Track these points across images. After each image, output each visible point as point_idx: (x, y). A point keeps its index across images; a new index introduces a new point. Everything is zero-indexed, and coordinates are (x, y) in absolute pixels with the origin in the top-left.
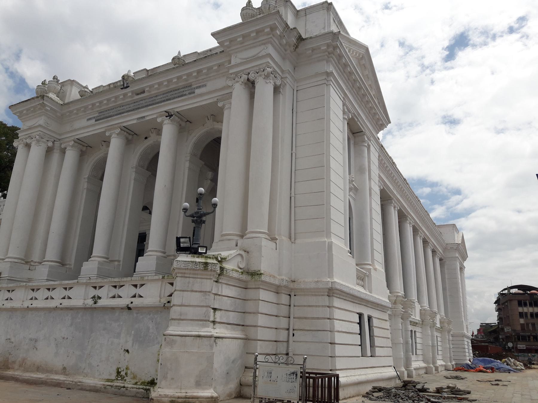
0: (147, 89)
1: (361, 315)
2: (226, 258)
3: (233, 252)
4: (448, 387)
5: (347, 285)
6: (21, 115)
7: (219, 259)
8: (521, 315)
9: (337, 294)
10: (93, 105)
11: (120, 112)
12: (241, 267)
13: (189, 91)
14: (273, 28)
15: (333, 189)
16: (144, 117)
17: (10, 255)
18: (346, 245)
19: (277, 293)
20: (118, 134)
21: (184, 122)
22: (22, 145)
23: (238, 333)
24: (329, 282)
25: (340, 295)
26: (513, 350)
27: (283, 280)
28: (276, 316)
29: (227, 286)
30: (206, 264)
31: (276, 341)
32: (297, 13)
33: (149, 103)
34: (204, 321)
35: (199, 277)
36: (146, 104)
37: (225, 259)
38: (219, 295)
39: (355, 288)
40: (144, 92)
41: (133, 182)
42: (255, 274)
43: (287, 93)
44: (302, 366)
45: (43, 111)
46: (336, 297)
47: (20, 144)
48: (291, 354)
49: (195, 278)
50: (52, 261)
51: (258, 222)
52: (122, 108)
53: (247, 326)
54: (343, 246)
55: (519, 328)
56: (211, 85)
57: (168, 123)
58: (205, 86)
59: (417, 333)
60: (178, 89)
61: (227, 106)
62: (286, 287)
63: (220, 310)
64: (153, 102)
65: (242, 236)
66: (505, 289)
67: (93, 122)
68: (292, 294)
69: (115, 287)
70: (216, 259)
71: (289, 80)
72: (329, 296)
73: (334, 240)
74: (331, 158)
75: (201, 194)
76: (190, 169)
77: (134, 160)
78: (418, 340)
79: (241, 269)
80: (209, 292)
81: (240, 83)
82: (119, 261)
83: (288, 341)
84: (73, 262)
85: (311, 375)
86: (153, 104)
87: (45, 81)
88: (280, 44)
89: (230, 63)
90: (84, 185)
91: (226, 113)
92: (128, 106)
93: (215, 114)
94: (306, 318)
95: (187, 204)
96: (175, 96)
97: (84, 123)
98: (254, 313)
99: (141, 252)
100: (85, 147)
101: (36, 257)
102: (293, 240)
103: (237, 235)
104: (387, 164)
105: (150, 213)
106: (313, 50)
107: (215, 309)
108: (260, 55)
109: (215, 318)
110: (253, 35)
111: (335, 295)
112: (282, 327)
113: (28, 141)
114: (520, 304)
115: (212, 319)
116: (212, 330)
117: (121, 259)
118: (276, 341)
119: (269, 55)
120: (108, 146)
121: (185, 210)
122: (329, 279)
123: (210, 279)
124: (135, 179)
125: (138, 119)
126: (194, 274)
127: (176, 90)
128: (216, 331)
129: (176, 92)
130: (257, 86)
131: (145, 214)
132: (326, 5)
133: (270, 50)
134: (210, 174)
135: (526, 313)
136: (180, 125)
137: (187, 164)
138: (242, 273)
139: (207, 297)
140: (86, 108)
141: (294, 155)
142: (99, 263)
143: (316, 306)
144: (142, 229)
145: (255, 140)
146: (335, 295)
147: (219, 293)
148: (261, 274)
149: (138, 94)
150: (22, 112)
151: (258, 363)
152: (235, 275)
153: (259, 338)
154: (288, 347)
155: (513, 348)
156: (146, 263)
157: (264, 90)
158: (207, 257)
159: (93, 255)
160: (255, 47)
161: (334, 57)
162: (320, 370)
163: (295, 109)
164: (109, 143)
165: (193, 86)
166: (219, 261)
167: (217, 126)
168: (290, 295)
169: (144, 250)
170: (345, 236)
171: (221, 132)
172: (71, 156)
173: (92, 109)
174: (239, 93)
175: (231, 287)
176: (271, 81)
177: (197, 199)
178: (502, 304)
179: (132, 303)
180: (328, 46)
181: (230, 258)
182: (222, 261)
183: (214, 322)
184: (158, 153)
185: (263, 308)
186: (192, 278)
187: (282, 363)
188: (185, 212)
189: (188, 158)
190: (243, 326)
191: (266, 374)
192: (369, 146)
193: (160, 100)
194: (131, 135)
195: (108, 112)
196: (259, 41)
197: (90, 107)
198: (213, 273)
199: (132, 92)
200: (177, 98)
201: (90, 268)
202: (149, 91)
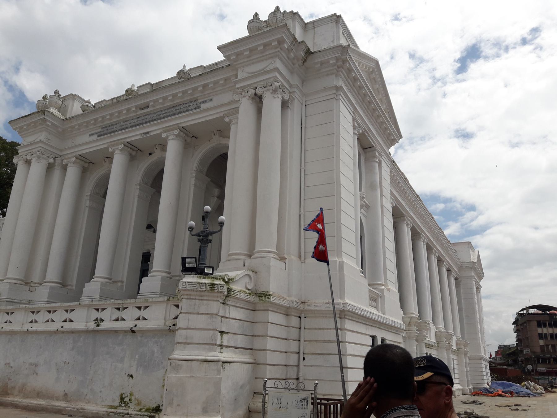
0: (151, 104)
2: (233, 279)
3: (241, 273)
4: (466, 413)
5: (359, 306)
6: (20, 131)
7: (227, 280)
8: (541, 336)
9: (349, 316)
10: (96, 120)
11: (123, 127)
12: (249, 288)
13: (195, 106)
14: (281, 42)
15: (344, 206)
16: (148, 133)
17: (9, 276)
18: (357, 264)
19: (287, 315)
20: (121, 150)
22: (22, 161)
23: (246, 358)
24: (340, 303)
25: (352, 317)
26: (532, 373)
27: (292, 301)
28: (286, 339)
29: (235, 308)
30: (213, 285)
31: (285, 366)
32: (305, 26)
34: (211, 345)
35: (205, 298)
36: (150, 119)
37: (232, 279)
38: (227, 318)
39: (367, 309)
40: (148, 107)
41: (136, 199)
42: (263, 295)
43: (296, 107)
44: (313, 392)
45: (44, 126)
46: (348, 319)
47: (19, 161)
48: (301, 379)
49: (202, 300)
51: (267, 241)
52: (125, 123)
53: (256, 350)
54: (355, 266)
55: (538, 350)
56: (217, 100)
57: (173, 139)
58: (211, 100)
60: (184, 104)
61: (234, 121)
62: (295, 308)
63: (228, 333)
64: (159, 117)
65: (250, 256)
66: (523, 309)
67: (95, 137)
68: (303, 316)
69: (118, 309)
70: (223, 279)
71: (297, 95)
72: (341, 318)
73: (345, 259)
74: (341, 175)
75: (207, 212)
76: (195, 186)
77: (138, 176)
79: (248, 290)
80: (216, 314)
81: (248, 97)
82: (122, 282)
83: (298, 366)
84: (74, 282)
85: (323, 401)
86: (158, 119)
87: (46, 95)
88: (288, 58)
89: (236, 76)
90: (86, 202)
91: (233, 128)
92: (131, 122)
93: (222, 130)
94: (317, 341)
95: (192, 223)
96: (181, 110)
97: (86, 138)
98: (262, 336)
99: (144, 272)
100: (87, 164)
101: (36, 278)
102: (303, 259)
103: (245, 255)
104: (399, 180)
105: (155, 231)
106: (322, 63)
107: (222, 333)
108: (268, 69)
109: (222, 342)
110: (261, 48)
111: (347, 317)
112: (292, 351)
113: (29, 157)
114: (539, 325)
115: (219, 343)
116: (219, 354)
117: (125, 279)
118: (285, 366)
119: (277, 69)
120: (111, 162)
121: (191, 229)
122: (340, 301)
123: (217, 301)
124: (139, 197)
125: (142, 134)
126: (200, 296)
127: (181, 105)
128: (223, 355)
129: (181, 107)
130: (265, 101)
131: (149, 232)
132: (335, 17)
133: (278, 64)
134: (216, 191)
135: (546, 334)
136: (186, 141)
137: (193, 181)
138: (250, 294)
139: (214, 319)
140: (88, 123)
141: (303, 171)
142: (102, 284)
143: (328, 329)
144: (147, 248)
146: (347, 317)
147: (227, 316)
148: (270, 295)
149: (142, 109)
150: (21, 128)
151: (267, 389)
152: (243, 296)
153: (268, 363)
154: (298, 371)
155: (532, 370)
156: (151, 284)
157: (272, 105)
158: (213, 278)
159: (96, 274)
160: (262, 61)
161: (343, 71)
162: (332, 395)
163: (303, 125)
164: (112, 159)
165: (199, 101)
166: (226, 282)
167: (223, 141)
168: (300, 317)
169: (148, 270)
170: (357, 255)
171: (227, 147)
172: (73, 173)
173: (94, 124)
174: (246, 108)
175: (239, 309)
176: (280, 96)
177: (203, 216)
178: (521, 325)
179: (136, 326)
180: (337, 59)
181: (237, 279)
182: (229, 281)
183: (221, 346)
184: (163, 169)
185: (272, 331)
186: (198, 299)
187: (292, 389)
188: (191, 231)
190: (251, 349)
191: (276, 400)
194: (134, 151)
195: (111, 127)
196: (266, 55)
197: (93, 122)
198: (219, 295)
199: (136, 107)
200: (182, 112)
201: (92, 289)
202: (153, 106)
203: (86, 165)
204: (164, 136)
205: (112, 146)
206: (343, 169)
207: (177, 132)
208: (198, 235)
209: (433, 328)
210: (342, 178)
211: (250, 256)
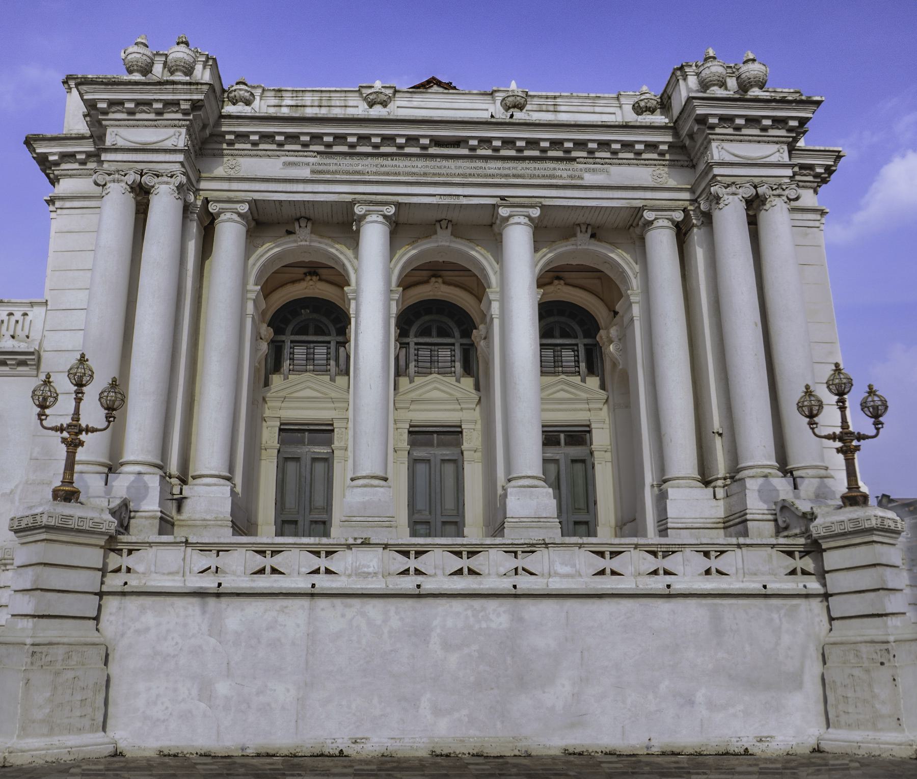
22: (123, 184)
33: (468, 171)
36: (460, 171)
57: (525, 224)
64: (480, 171)
96: (537, 172)
172: (230, 234)
193: (497, 171)
207: (536, 213)
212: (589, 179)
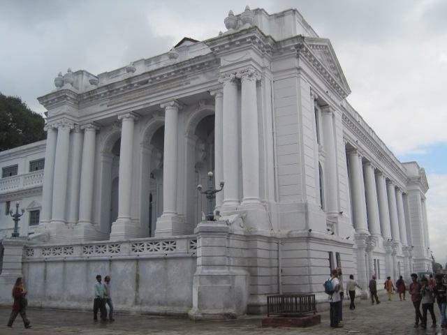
0: (150, 81)
1: (330, 253)
6: (46, 105)
14: (253, 38)
16: (148, 103)
21: (183, 106)
41: (141, 155)
50: (86, 222)
59: (380, 262)
61: (218, 95)
71: (268, 75)
77: (141, 137)
78: (381, 267)
82: (138, 220)
88: (259, 48)
90: (101, 158)
93: (208, 99)
97: (97, 108)
100: (100, 127)
103: (236, 201)
104: (352, 121)
106: (285, 49)
108: (244, 59)
145: (243, 120)
150: (47, 102)
167: (209, 108)
172: (90, 135)
174: (229, 89)
180: (297, 46)
189: (187, 135)
192: (333, 115)
194: (139, 117)
203: (98, 128)
204: (162, 106)
205: (120, 115)
206: (305, 131)
207: (172, 103)
208: (206, 193)
209: (381, 240)
210: (305, 138)
211: (240, 202)
212: (193, 83)
